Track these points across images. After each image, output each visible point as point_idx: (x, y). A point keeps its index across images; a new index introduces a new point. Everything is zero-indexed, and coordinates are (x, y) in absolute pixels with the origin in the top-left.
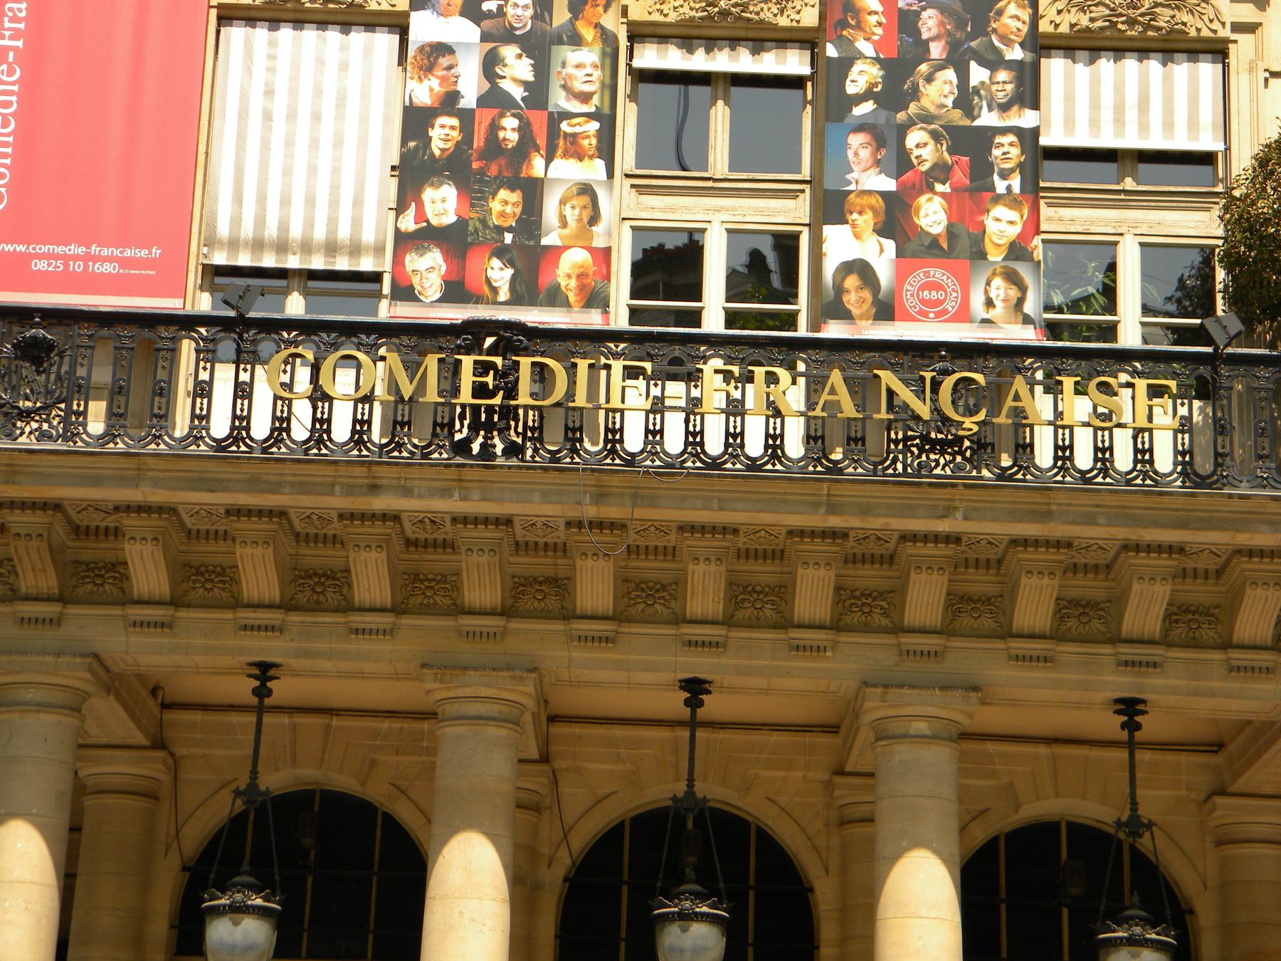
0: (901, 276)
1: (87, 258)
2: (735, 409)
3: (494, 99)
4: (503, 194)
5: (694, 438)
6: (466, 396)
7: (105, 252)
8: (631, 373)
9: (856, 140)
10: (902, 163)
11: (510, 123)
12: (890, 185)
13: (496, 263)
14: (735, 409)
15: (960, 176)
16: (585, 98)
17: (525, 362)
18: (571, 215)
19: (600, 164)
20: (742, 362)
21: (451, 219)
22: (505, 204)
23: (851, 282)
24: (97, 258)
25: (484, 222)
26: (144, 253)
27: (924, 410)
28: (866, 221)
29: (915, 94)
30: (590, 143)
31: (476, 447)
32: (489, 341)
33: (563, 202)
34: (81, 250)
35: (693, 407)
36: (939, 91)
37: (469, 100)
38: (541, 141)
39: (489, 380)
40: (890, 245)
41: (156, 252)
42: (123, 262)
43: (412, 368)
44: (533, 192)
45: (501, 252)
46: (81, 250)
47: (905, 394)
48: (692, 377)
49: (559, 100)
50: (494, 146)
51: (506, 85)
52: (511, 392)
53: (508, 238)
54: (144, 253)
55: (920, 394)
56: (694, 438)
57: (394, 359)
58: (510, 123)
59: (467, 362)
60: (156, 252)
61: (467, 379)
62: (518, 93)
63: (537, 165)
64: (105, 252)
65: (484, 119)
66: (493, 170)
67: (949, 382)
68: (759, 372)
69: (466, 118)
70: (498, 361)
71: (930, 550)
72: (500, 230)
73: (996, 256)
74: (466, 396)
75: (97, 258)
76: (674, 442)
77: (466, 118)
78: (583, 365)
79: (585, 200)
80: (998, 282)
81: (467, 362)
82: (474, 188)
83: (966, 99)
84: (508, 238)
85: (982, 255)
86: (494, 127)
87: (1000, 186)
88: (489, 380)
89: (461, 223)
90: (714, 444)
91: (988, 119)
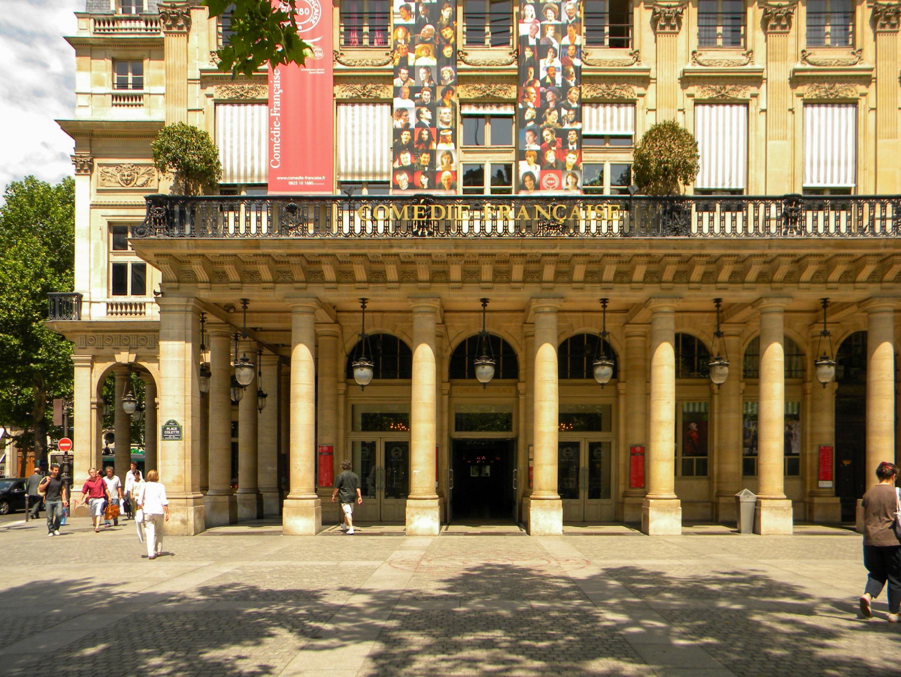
0: (542, 176)
1: (304, 180)
2: (494, 219)
3: (420, 125)
4: (424, 155)
5: (483, 228)
6: (416, 218)
8: (464, 209)
9: (528, 134)
10: (542, 141)
12: (538, 148)
13: (423, 177)
14: (494, 219)
15: (559, 144)
16: (447, 123)
17: (433, 207)
18: (445, 161)
19: (453, 144)
20: (496, 204)
21: (409, 163)
22: (425, 158)
23: (527, 178)
24: (307, 180)
27: (548, 217)
28: (531, 159)
29: (545, 119)
30: (449, 138)
31: (420, 233)
32: (422, 201)
35: (482, 219)
36: (552, 118)
37: (413, 125)
38: (435, 138)
39: (423, 212)
40: (539, 167)
42: (315, 181)
43: (400, 210)
44: (433, 154)
45: (424, 173)
47: (543, 212)
48: (482, 210)
49: (440, 125)
50: (421, 140)
51: (423, 120)
52: (429, 216)
53: (426, 169)
54: (320, 178)
55: (547, 212)
56: (483, 228)
57: (395, 207)
58: (425, 132)
59: (416, 207)
61: (416, 213)
63: (434, 144)
65: (417, 132)
66: (421, 148)
67: (556, 208)
68: (501, 207)
70: (425, 207)
71: (550, 258)
72: (424, 166)
73: (569, 169)
74: (416, 218)
75: (307, 180)
76: (477, 229)
78: (450, 207)
80: (570, 177)
81: (416, 207)
82: (415, 153)
83: (560, 120)
84: (426, 169)
85: (565, 169)
86: (420, 134)
87: (571, 147)
89: (412, 164)
90: (488, 230)
91: (567, 126)
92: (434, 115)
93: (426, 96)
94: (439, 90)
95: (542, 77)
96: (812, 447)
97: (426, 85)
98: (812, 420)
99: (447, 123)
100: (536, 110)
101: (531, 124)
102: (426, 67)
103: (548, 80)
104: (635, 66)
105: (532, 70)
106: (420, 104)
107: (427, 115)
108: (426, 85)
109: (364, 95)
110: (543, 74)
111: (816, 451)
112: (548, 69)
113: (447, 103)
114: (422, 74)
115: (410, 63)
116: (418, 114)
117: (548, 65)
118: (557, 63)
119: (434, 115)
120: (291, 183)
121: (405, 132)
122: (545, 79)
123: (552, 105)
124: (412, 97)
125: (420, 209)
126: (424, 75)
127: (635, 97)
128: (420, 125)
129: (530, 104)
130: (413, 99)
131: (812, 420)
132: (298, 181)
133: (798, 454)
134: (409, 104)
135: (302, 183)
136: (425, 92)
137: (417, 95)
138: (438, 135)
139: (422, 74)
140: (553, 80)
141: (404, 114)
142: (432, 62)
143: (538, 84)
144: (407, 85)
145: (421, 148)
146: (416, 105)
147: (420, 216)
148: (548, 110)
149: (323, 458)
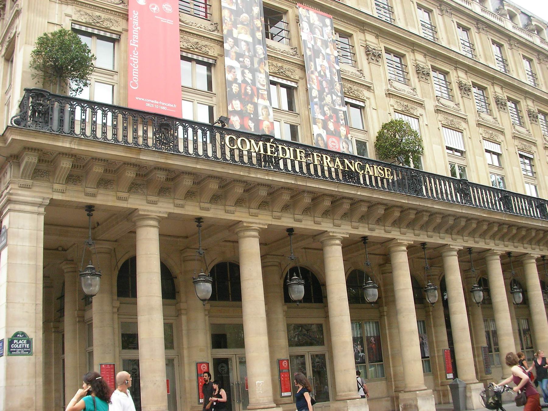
0: (328, 139)
1: (159, 105)
3: (244, 81)
4: (249, 105)
6: (269, 153)
7: (163, 104)
9: (316, 107)
10: (324, 114)
11: (249, 88)
12: (323, 118)
13: (250, 122)
15: (334, 118)
16: (264, 86)
18: (264, 113)
19: (268, 102)
21: (239, 109)
22: (250, 107)
23: (319, 138)
24: (162, 105)
25: (246, 111)
26: (172, 106)
28: (320, 125)
30: (266, 96)
33: (262, 109)
34: (157, 102)
36: (328, 99)
37: (240, 81)
38: (256, 94)
39: (273, 149)
40: (325, 131)
41: (175, 106)
42: (168, 107)
44: (256, 105)
45: (251, 119)
46: (157, 102)
49: (258, 85)
50: (246, 93)
53: (252, 116)
54: (172, 106)
59: (268, 144)
60: (175, 106)
62: (250, 82)
63: (256, 99)
64: (163, 104)
65: (243, 86)
66: (247, 99)
69: (239, 84)
73: (343, 138)
74: (269, 153)
75: (162, 105)
77: (240, 85)
79: (265, 110)
80: (344, 143)
82: (244, 103)
83: (333, 102)
84: (252, 116)
85: (341, 137)
86: (246, 89)
87: (342, 122)
88: (273, 149)
89: (241, 110)
91: (337, 107)
92: (254, 76)
93: (247, 62)
94: (256, 60)
95: (318, 70)
96: (438, 351)
97: (247, 54)
98: (436, 333)
99: (264, 86)
100: (318, 91)
101: (316, 100)
102: (245, 41)
103: (322, 73)
104: (362, 79)
105: (312, 64)
106: (244, 67)
107: (249, 76)
108: (247, 54)
109: (197, 48)
110: (319, 69)
111: (441, 353)
112: (321, 66)
113: (262, 71)
114: (243, 46)
115: (235, 35)
116: (243, 73)
117: (321, 63)
118: (325, 64)
119: (254, 76)
120: (148, 105)
121: (234, 85)
122: (320, 71)
123: (326, 90)
124: (237, 59)
125: (271, 146)
126: (245, 47)
127: (365, 99)
128: (244, 81)
129: (315, 87)
130: (239, 62)
131: (436, 333)
132: (154, 104)
133: (428, 357)
134: (236, 64)
135: (157, 107)
136: (246, 59)
137: (241, 59)
138: (258, 92)
139: (243, 46)
140: (325, 73)
141: (233, 70)
142: (250, 40)
143: (316, 74)
144: (233, 50)
145: (247, 99)
146: (241, 67)
148: (325, 93)
149: (388, 358)
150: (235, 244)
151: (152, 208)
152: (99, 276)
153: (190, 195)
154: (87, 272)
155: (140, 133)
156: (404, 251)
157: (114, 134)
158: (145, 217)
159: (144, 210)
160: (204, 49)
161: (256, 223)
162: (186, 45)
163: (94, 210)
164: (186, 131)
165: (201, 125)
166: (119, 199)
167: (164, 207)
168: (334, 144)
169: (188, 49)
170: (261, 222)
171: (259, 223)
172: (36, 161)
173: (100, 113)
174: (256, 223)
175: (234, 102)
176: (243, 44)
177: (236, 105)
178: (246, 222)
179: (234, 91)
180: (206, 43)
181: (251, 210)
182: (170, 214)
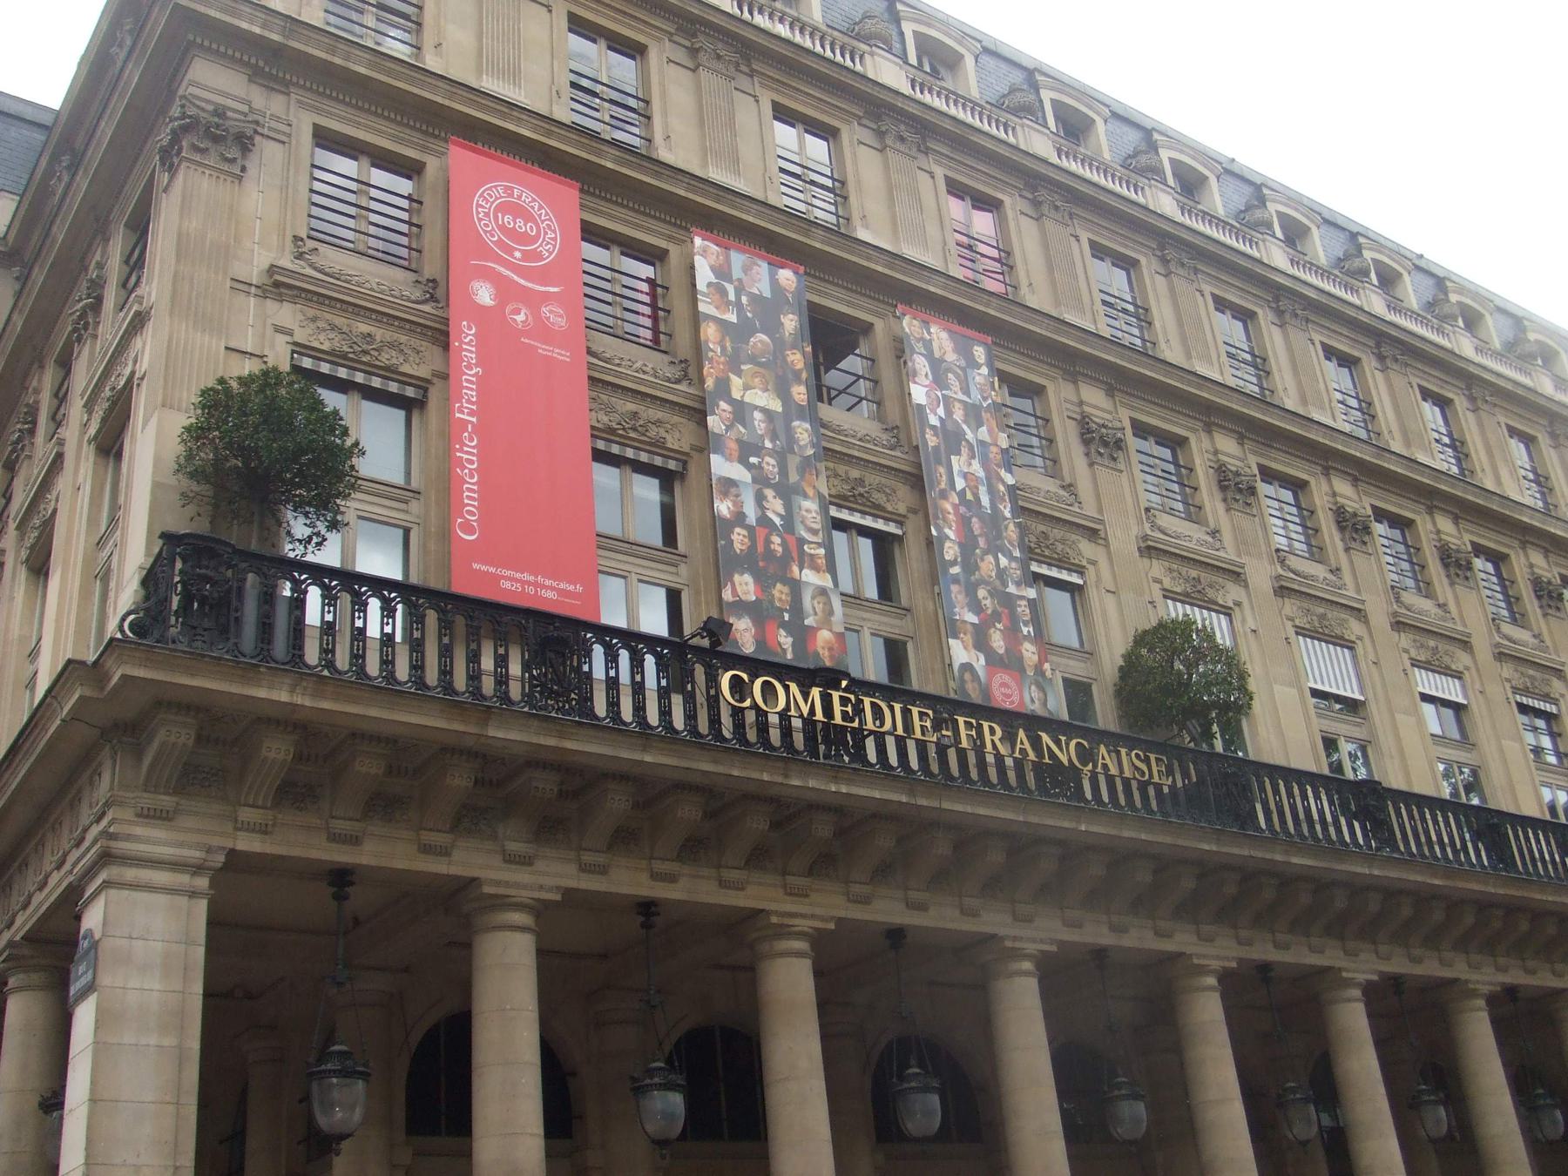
0: (990, 676)
1: (536, 585)
4: (779, 586)
6: (838, 720)
7: (548, 583)
9: (954, 588)
10: (977, 607)
11: (776, 540)
13: (782, 632)
18: (819, 608)
22: (780, 592)
24: (544, 587)
25: (772, 602)
26: (571, 588)
28: (969, 639)
29: (978, 568)
30: (822, 562)
32: (844, 683)
33: (813, 598)
34: (532, 578)
36: (987, 566)
38: (795, 555)
41: (579, 588)
42: (561, 592)
44: (796, 587)
45: (784, 625)
46: (532, 578)
50: (769, 553)
51: (770, 515)
54: (571, 588)
58: (776, 540)
59: (836, 695)
60: (579, 588)
62: (777, 521)
63: (795, 569)
64: (548, 583)
65: (761, 533)
69: (749, 528)
72: (782, 610)
74: (838, 720)
75: (544, 587)
77: (749, 528)
79: (822, 599)
83: (1001, 573)
86: (768, 542)
87: (1025, 630)
88: (849, 709)
91: (1012, 589)
93: (770, 465)
94: (793, 462)
97: (768, 444)
99: (815, 532)
100: (961, 545)
102: (764, 410)
103: (969, 496)
105: (942, 470)
106: (761, 480)
107: (775, 506)
108: (768, 444)
109: (634, 429)
110: (960, 484)
112: (965, 476)
113: (810, 492)
115: (736, 395)
116: (760, 499)
118: (976, 468)
119: (788, 506)
120: (506, 585)
121: (738, 530)
123: (982, 542)
127: (1084, 563)
128: (764, 521)
129: (951, 534)
130: (749, 467)
132: (523, 582)
135: (531, 590)
136: (767, 459)
137: (753, 460)
138: (802, 553)
140: (976, 496)
141: (733, 490)
142: (776, 406)
144: (732, 434)
146: (755, 480)
147: (845, 715)
150: (745, 976)
151: (521, 876)
152: (365, 1076)
153: (624, 839)
154: (329, 1066)
155: (487, 663)
156: (1211, 988)
157: (413, 667)
158: (501, 903)
159: (498, 883)
160: (653, 432)
161: (803, 916)
162: (606, 419)
163: (352, 884)
164: (612, 658)
165: (652, 641)
166: (426, 849)
167: (555, 874)
168: (1009, 692)
169: (612, 431)
170: (818, 911)
171: (813, 917)
172: (191, 743)
173: (374, 605)
174: (803, 916)
175: (737, 578)
176: (757, 415)
177: (745, 586)
178: (777, 913)
179: (738, 547)
180: (660, 415)
181: (790, 879)
182: (568, 893)
